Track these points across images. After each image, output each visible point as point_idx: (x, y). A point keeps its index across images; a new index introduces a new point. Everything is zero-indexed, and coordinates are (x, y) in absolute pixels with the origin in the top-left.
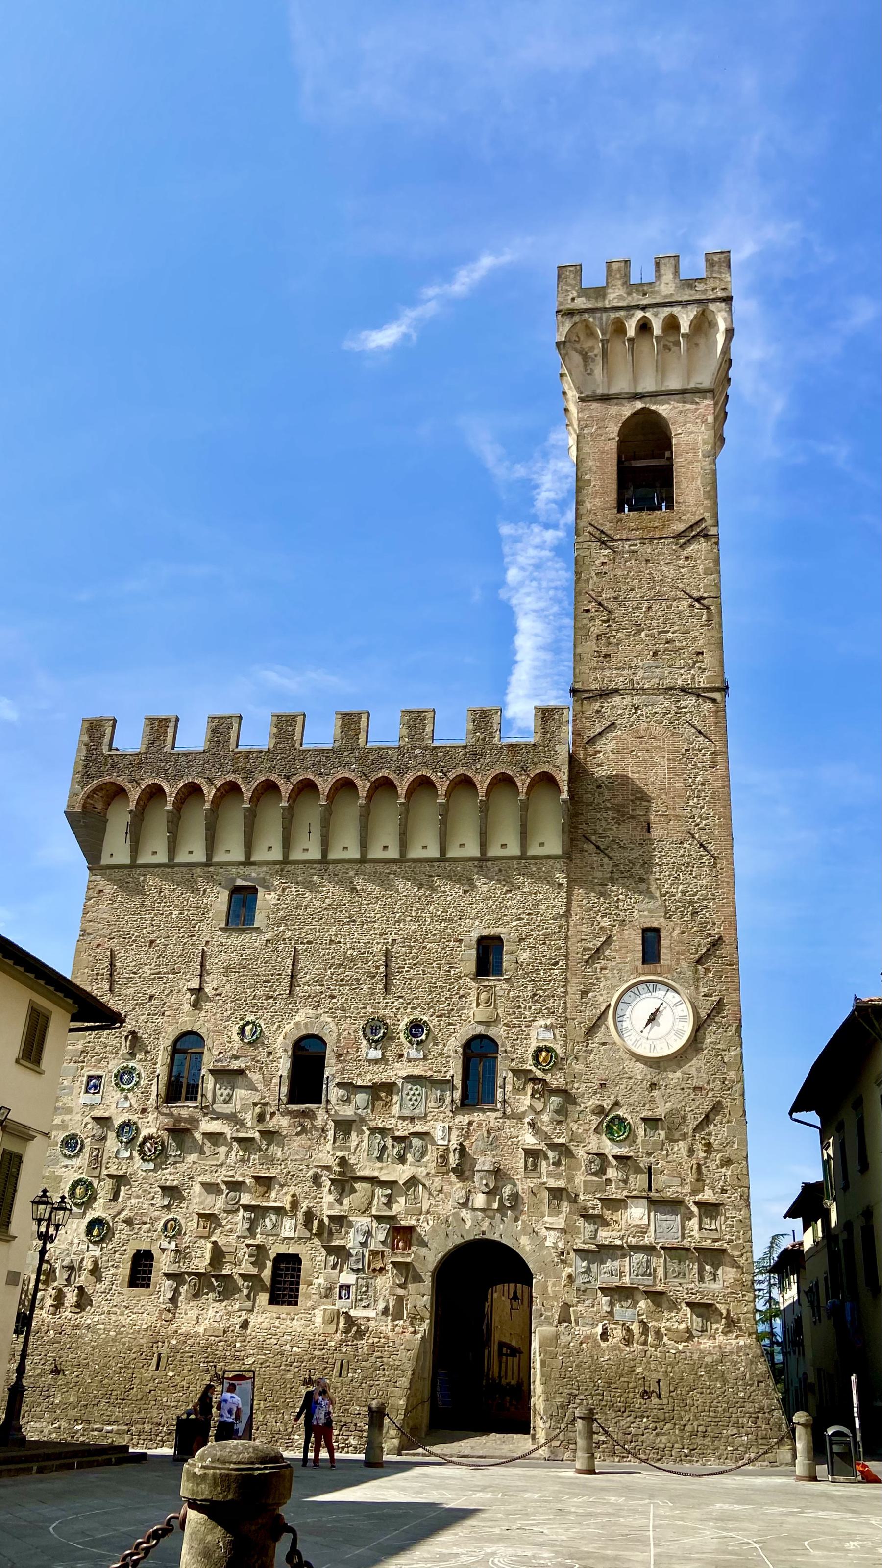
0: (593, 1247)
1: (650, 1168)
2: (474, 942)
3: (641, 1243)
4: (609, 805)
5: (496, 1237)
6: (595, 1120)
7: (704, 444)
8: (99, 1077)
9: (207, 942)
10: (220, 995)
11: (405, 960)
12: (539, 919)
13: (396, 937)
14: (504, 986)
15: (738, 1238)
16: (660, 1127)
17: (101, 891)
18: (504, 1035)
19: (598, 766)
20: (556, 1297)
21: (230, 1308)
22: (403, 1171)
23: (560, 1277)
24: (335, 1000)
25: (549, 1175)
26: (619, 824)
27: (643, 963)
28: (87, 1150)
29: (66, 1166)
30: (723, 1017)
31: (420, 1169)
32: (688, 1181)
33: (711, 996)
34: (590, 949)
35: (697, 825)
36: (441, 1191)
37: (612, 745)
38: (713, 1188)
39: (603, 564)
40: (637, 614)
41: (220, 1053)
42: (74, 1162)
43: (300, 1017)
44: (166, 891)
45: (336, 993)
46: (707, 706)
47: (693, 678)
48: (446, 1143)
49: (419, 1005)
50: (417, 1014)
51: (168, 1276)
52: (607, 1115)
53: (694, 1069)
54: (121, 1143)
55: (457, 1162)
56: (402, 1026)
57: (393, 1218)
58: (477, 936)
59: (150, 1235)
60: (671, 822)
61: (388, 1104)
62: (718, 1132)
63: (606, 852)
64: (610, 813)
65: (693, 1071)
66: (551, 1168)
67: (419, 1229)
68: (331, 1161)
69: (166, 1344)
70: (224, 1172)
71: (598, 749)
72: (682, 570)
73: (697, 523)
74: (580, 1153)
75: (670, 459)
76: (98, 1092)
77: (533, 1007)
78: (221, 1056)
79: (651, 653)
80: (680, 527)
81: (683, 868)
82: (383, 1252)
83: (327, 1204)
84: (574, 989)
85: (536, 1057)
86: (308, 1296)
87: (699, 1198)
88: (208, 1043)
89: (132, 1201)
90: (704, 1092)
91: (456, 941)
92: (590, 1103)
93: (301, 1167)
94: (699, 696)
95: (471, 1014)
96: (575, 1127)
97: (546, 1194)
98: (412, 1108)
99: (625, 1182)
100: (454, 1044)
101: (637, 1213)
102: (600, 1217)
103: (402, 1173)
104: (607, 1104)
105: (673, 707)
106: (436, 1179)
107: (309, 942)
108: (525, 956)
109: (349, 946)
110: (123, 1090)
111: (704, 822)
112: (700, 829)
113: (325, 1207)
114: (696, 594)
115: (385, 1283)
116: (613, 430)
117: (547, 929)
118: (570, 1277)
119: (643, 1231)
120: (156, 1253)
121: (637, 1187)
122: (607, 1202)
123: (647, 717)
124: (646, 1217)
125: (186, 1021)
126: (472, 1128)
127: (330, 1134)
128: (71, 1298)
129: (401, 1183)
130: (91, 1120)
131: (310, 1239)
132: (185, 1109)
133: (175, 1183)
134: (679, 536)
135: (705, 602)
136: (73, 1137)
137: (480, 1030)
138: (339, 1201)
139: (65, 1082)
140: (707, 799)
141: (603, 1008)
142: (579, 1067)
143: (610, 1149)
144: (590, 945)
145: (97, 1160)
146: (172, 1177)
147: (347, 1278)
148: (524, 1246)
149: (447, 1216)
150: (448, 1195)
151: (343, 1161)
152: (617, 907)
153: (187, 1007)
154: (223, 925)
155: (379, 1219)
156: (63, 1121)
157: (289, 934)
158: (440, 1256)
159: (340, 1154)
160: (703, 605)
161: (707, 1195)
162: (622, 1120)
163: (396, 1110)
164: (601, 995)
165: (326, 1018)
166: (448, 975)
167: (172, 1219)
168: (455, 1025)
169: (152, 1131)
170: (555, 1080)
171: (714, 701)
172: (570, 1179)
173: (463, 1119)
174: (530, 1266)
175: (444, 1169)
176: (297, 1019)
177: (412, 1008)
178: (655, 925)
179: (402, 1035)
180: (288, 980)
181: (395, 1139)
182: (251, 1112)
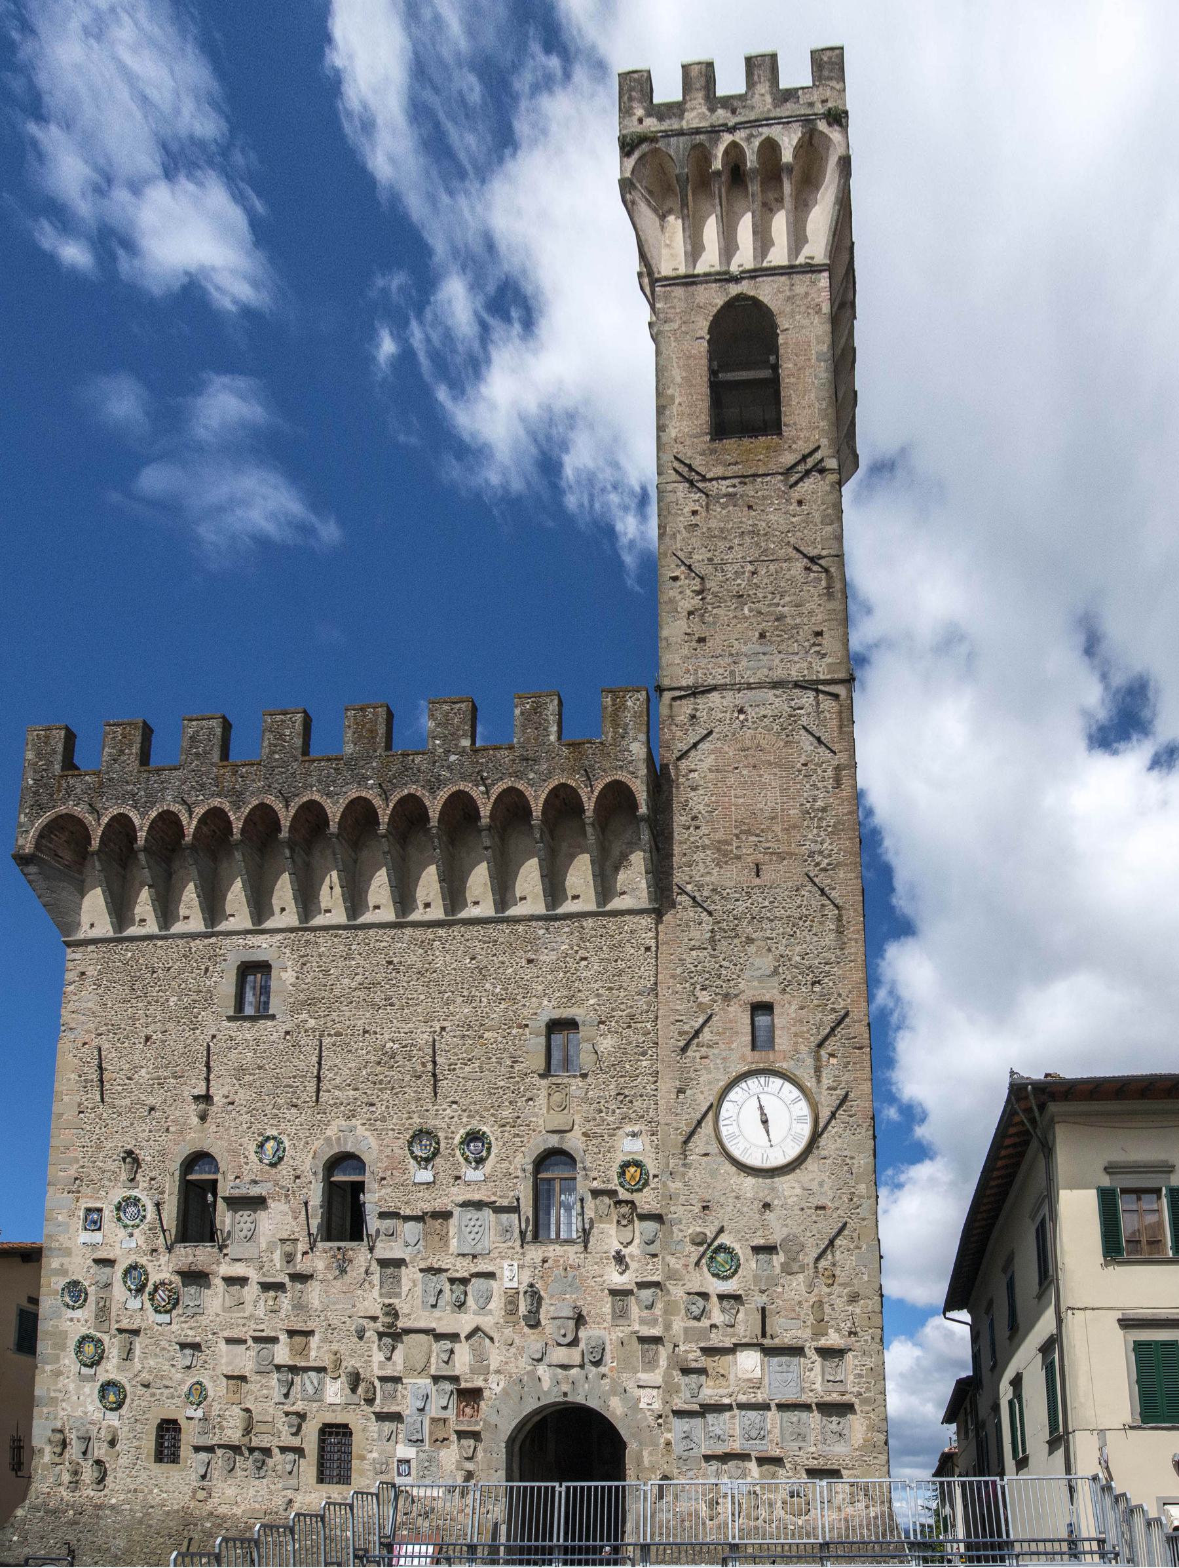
0: (696, 1408)
1: (763, 1309)
2: (543, 1025)
3: (753, 1400)
4: (707, 842)
5: (580, 1399)
6: (695, 1252)
7: (818, 343)
8: (100, 1210)
9: (214, 1037)
10: (232, 1104)
11: (456, 1055)
12: (622, 994)
13: (445, 1024)
14: (580, 1084)
15: (868, 1389)
17: (83, 974)
18: (583, 1146)
19: (694, 789)
20: (653, 1469)
21: (272, 1487)
23: (658, 1445)
24: (373, 1109)
25: (643, 1321)
26: (721, 867)
27: (753, 1049)
28: (92, 1299)
29: (71, 1320)
30: (851, 1116)
32: (809, 1323)
33: (835, 1089)
34: (686, 1033)
35: (818, 864)
37: (710, 761)
38: (838, 1330)
39: (694, 513)
40: (739, 581)
41: (237, 1177)
42: (78, 1314)
43: (331, 1132)
44: (160, 971)
45: (374, 1099)
46: (827, 704)
47: (810, 668)
49: (477, 1112)
50: (475, 1124)
51: (197, 1449)
52: (710, 1245)
53: (816, 1182)
54: (130, 1290)
56: (457, 1140)
57: (455, 1379)
58: (547, 1019)
59: (174, 1401)
60: (785, 862)
61: (444, 1238)
62: (845, 1258)
63: (705, 905)
64: (709, 852)
65: (815, 1186)
68: (377, 1311)
69: (199, 1528)
70: (254, 1326)
71: (693, 767)
72: (794, 520)
73: (811, 454)
74: (677, 1292)
75: (776, 367)
76: (99, 1229)
77: (618, 1111)
78: (238, 1180)
79: (757, 635)
80: (789, 459)
81: (801, 923)
83: (375, 1361)
84: (667, 1086)
85: (622, 1174)
86: (362, 1473)
87: (823, 1342)
88: (222, 1166)
89: (147, 1358)
90: (828, 1212)
91: (519, 1026)
92: (690, 1231)
94: (817, 691)
95: (541, 1122)
96: (672, 1261)
98: (473, 1243)
100: (523, 1161)
101: (749, 1362)
103: (464, 1323)
104: (710, 1233)
105: (786, 707)
107: (338, 1034)
108: (606, 1044)
109: (386, 1036)
110: (125, 1227)
111: (826, 861)
112: (821, 870)
113: (375, 1366)
114: (812, 552)
115: (450, 1455)
116: (702, 325)
117: (631, 1007)
118: (668, 1444)
119: (757, 1385)
120: (183, 1423)
122: (708, 1351)
123: (754, 723)
124: (759, 1368)
125: (195, 1138)
126: (546, 1265)
127: (376, 1279)
128: (88, 1474)
129: (463, 1336)
130: (92, 1264)
132: (199, 1255)
133: (198, 1339)
134: (789, 471)
135: (822, 562)
136: (75, 1283)
137: (553, 1141)
139: (60, 1217)
140: (830, 829)
141: (704, 1109)
142: (675, 1186)
144: (686, 1028)
145: (103, 1313)
146: (191, 1333)
147: (404, 1451)
148: (615, 1409)
149: (518, 1376)
150: (521, 1350)
152: (719, 977)
153: (195, 1120)
154: (231, 1013)
155: (436, 1379)
156: (62, 1265)
157: (312, 1023)
158: (517, 1421)
159: (387, 1301)
160: (821, 566)
161: (833, 1339)
163: (454, 1244)
164: (702, 1092)
165: (361, 1130)
166: (510, 1073)
167: (197, 1383)
168: (522, 1136)
169: (165, 1276)
170: (646, 1200)
171: (836, 696)
172: (668, 1327)
173: (535, 1253)
174: (622, 1432)
175: (512, 1318)
176: (328, 1133)
177: (469, 1117)
178: (767, 998)
179: (458, 1152)
180: (314, 1084)
181: (452, 1281)
182: (278, 1252)
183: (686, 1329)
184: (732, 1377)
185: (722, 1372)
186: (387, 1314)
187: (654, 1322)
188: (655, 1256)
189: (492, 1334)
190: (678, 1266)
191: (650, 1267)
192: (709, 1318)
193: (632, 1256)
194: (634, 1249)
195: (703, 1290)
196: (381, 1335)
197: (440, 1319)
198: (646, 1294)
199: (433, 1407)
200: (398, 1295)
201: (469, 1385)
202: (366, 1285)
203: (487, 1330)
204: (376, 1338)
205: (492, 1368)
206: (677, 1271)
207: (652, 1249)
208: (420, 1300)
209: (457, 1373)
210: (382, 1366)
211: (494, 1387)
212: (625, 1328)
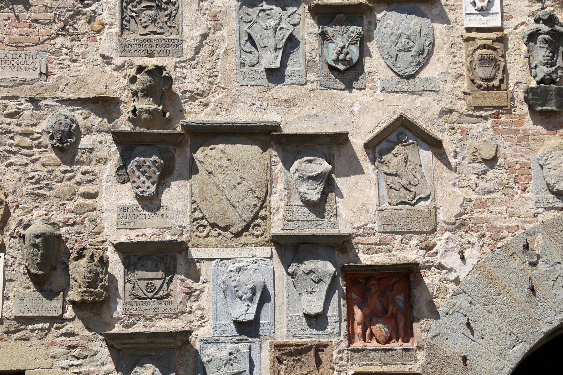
22: (365, 109)
31: (419, 100)
36: (491, 162)
48: (494, 21)
55: (542, 71)
67: (430, 279)
82: (319, 348)
83: (111, 208)
93: (12, 106)
103: (362, 113)
106: (476, 128)
129: (358, 142)
131: (61, 320)
138: (150, 203)
151: (159, 84)
155: (292, 249)
186: (147, 92)
189: (435, 132)
196: (128, 145)
197: (290, 103)
199: (282, 316)
200: (173, 47)
201: (379, 258)
202: (81, 24)
203: (423, 124)
204: (112, 152)
205: (442, 216)
208: (234, 60)
209: (344, 229)
210: (125, 219)
211: (452, 267)
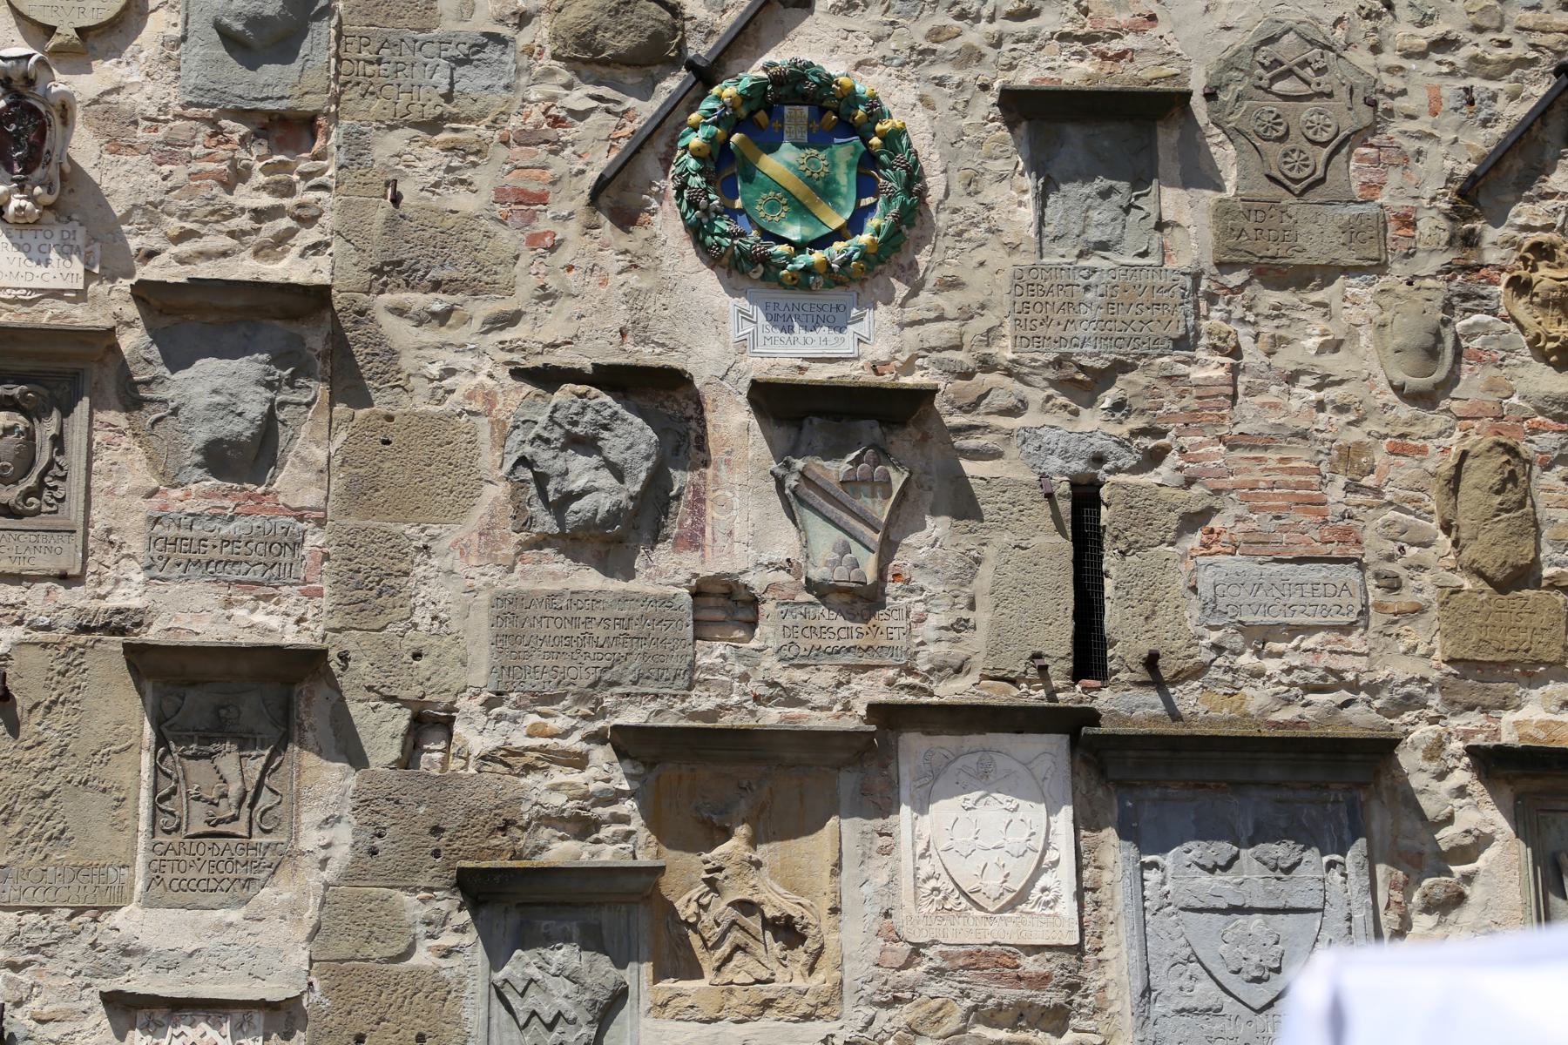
16: (1166, 158)
25: (175, 552)
52: (705, 76)
66: (200, 492)
74: (454, 369)
97: (119, 711)
99: (863, 601)
102: (639, 888)
121: (975, 643)
124: (1062, 880)
143: (728, 341)
162: (829, 110)
172: (373, 587)
183: (509, 608)
184: (853, 943)
185: (777, 901)
187: (265, 564)
188: (289, 129)
190: (462, 201)
191: (249, 197)
192: (693, 541)
193: (119, 128)
194: (135, 77)
195: (648, 356)
198: (219, 388)
206: (452, 234)
207: (275, 85)
212: (38, 600)
